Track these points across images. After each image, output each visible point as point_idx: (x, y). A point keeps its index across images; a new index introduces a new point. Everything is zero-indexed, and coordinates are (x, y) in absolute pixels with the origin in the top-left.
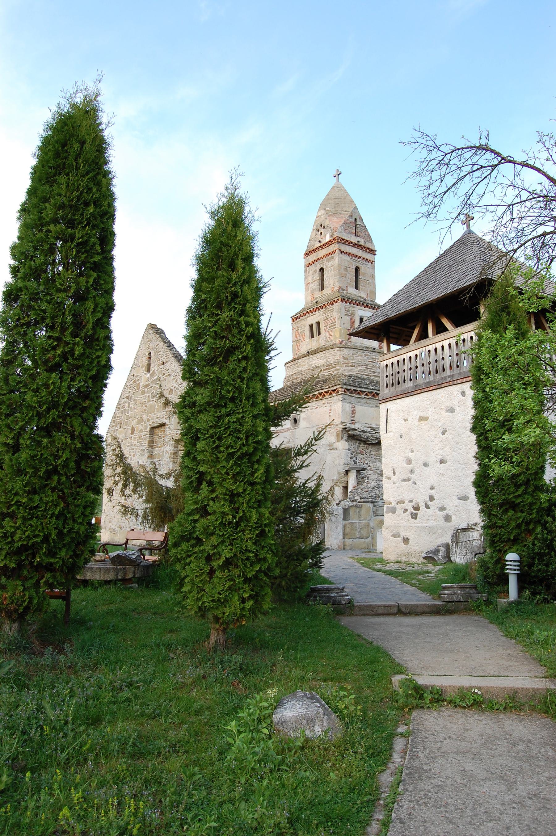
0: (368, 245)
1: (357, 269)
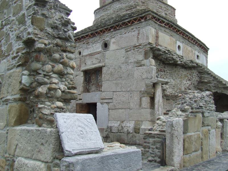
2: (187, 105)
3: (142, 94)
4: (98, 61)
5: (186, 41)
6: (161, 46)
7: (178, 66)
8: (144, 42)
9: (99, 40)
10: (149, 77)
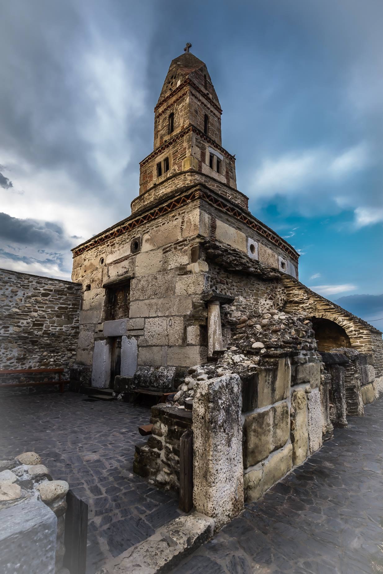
0: (214, 101)
1: (206, 118)
2: (257, 340)
3: (188, 320)
4: (125, 270)
5: (264, 239)
6: (220, 242)
7: (251, 277)
8: (191, 234)
9: (128, 239)
10: (198, 292)
